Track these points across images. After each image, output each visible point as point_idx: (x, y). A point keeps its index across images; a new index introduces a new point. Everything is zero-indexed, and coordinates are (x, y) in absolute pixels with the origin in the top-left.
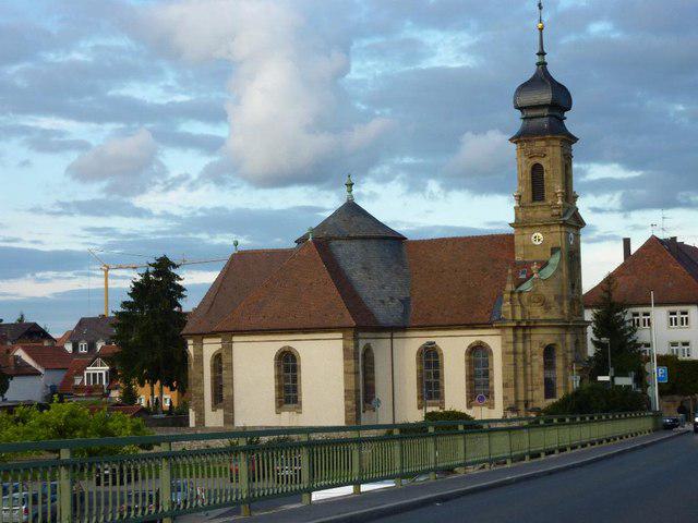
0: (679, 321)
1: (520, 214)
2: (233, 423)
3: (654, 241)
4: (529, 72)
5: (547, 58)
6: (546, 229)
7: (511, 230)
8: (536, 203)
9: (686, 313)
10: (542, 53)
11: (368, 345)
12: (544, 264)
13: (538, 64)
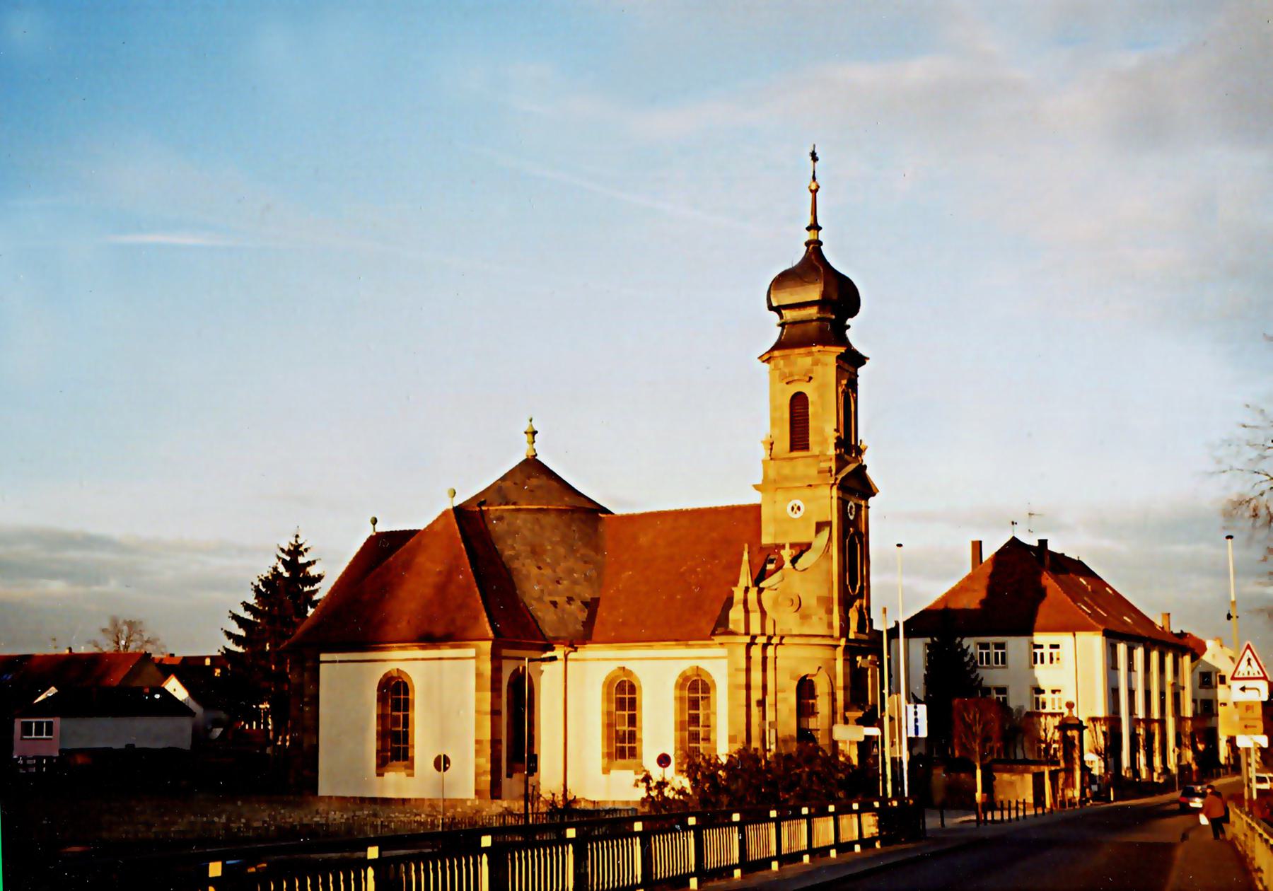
0: (1047, 658)
1: (772, 474)
4: (795, 255)
5: (822, 236)
6: (808, 492)
8: (795, 454)
9: (1057, 647)
10: (815, 227)
12: (803, 548)
13: (808, 244)
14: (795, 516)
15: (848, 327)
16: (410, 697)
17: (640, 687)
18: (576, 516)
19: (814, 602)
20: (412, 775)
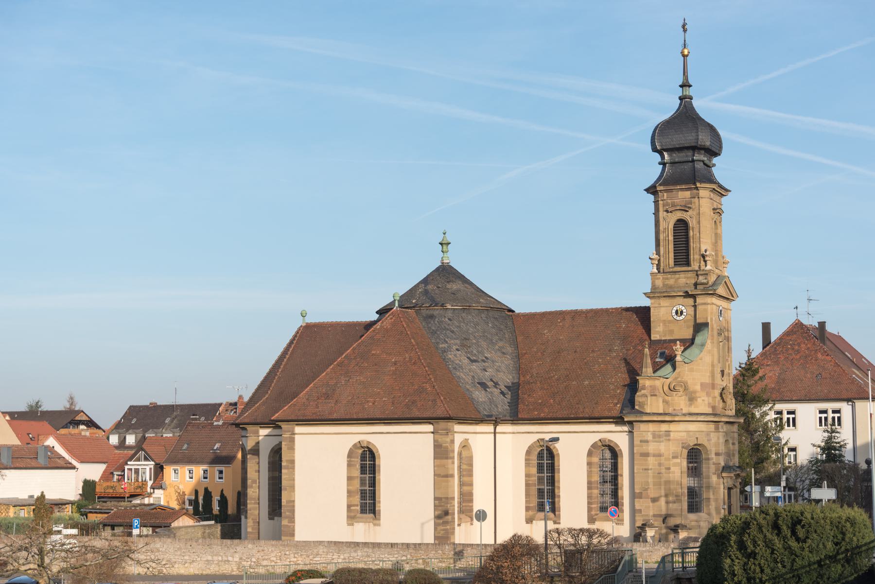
2: (293, 535)
3: (798, 328)
4: (670, 106)
5: (690, 92)
7: (646, 302)
10: (685, 85)
11: (467, 440)
14: (678, 318)
15: (714, 165)
16: (377, 463)
17: (558, 454)
18: (491, 313)
19: (698, 388)
20: (379, 525)
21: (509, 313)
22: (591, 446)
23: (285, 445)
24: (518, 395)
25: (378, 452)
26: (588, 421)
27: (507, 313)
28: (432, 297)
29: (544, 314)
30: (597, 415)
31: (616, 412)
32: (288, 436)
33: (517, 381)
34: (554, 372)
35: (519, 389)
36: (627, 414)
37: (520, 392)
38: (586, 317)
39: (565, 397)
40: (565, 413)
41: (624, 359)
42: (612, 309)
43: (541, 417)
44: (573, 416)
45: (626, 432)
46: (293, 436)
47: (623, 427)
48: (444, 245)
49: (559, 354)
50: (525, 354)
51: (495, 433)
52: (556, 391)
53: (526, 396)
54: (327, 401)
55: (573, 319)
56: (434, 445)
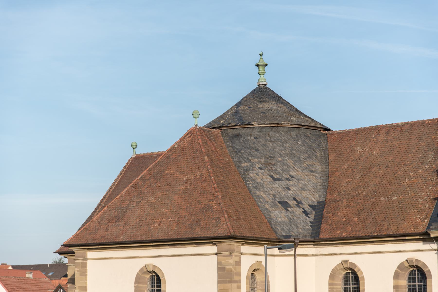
17: (363, 278)
18: (302, 131)
21: (324, 132)
22: (398, 268)
23: (78, 271)
24: (323, 214)
25: (163, 276)
26: (393, 239)
27: (321, 131)
28: (241, 116)
29: (358, 131)
30: (401, 232)
31: (422, 229)
32: (81, 261)
33: (324, 199)
34: (363, 189)
35: (324, 208)
36: (433, 229)
37: (325, 211)
38: (401, 131)
39: (370, 214)
40: (368, 232)
41: (436, 171)
42: (428, 120)
43: (343, 236)
44: (376, 234)
45: (435, 250)
46: (85, 261)
47: (431, 245)
48: (260, 67)
49: (370, 170)
50: (336, 171)
51: (295, 256)
52: (362, 208)
53: (330, 215)
54: (117, 223)
55: (388, 134)
56: (218, 267)
